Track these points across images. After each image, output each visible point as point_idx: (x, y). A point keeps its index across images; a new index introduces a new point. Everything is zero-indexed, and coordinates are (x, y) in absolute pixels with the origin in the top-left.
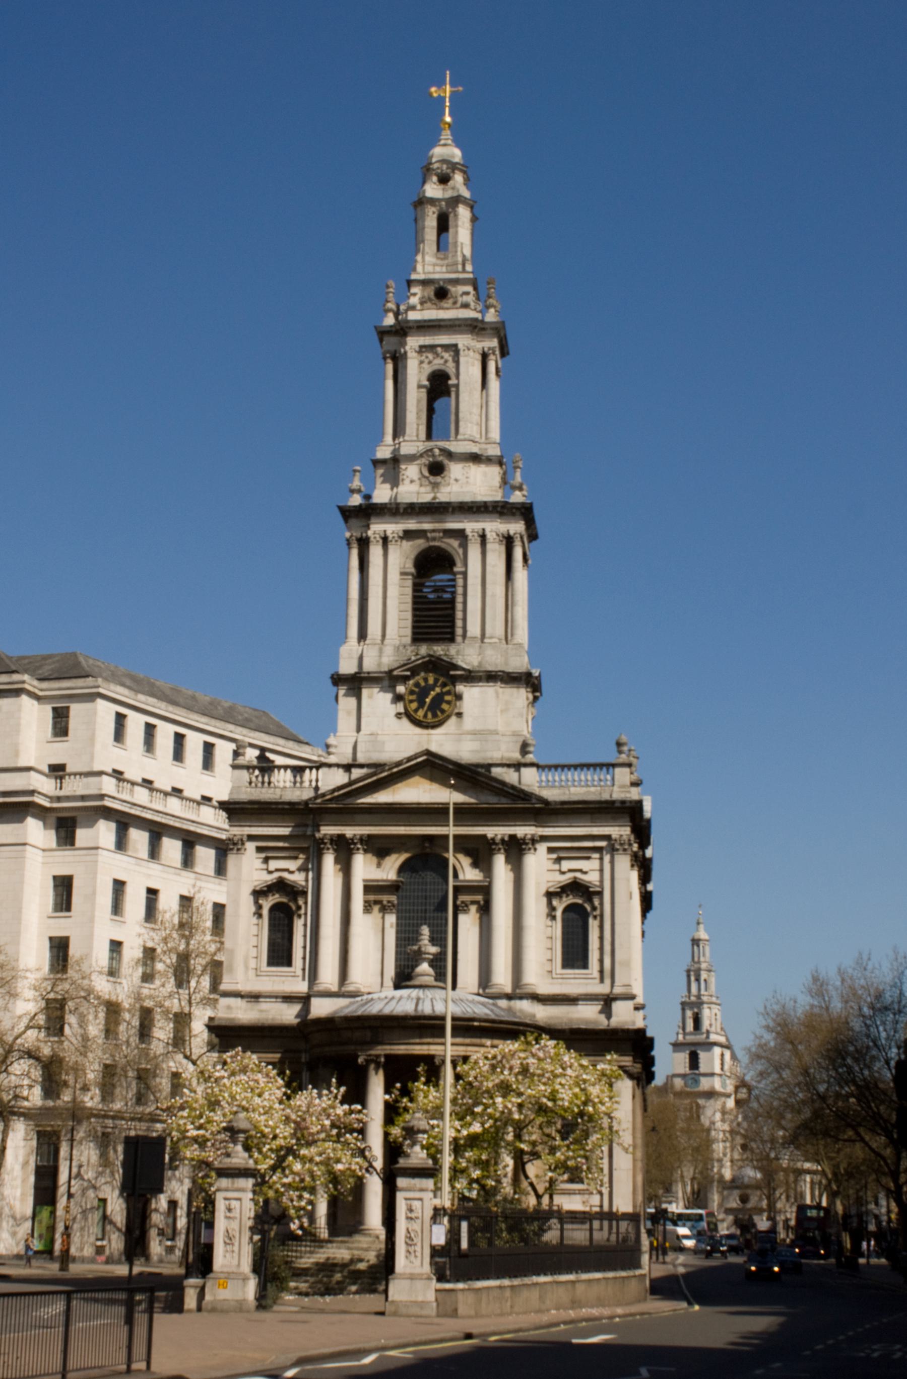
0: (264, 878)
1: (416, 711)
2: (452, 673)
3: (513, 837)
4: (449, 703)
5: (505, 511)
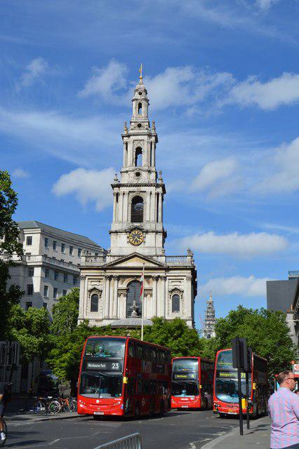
0: (91, 287)
3: (159, 276)
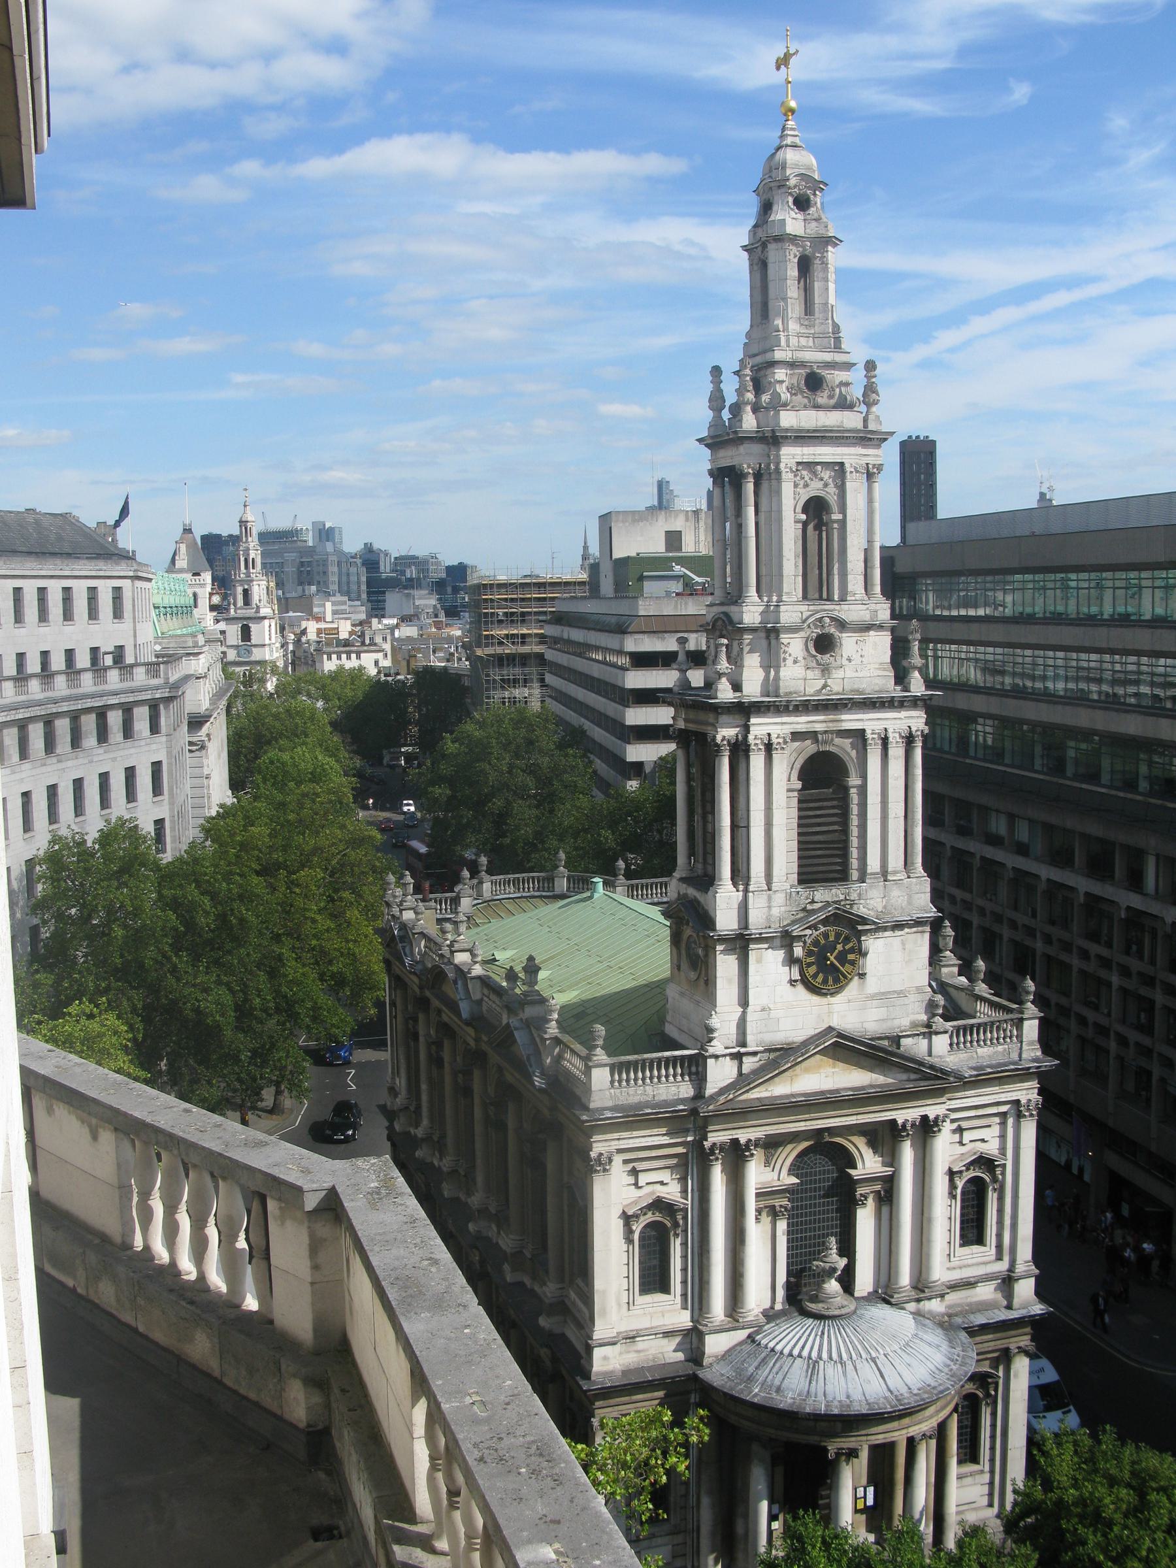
1: (815, 976)
2: (860, 928)
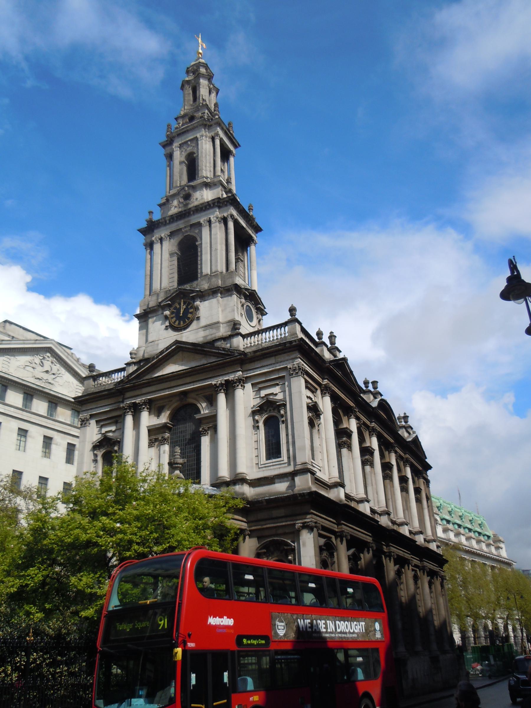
1: (175, 322)
2: (191, 295)
4: (191, 313)
5: (221, 205)
